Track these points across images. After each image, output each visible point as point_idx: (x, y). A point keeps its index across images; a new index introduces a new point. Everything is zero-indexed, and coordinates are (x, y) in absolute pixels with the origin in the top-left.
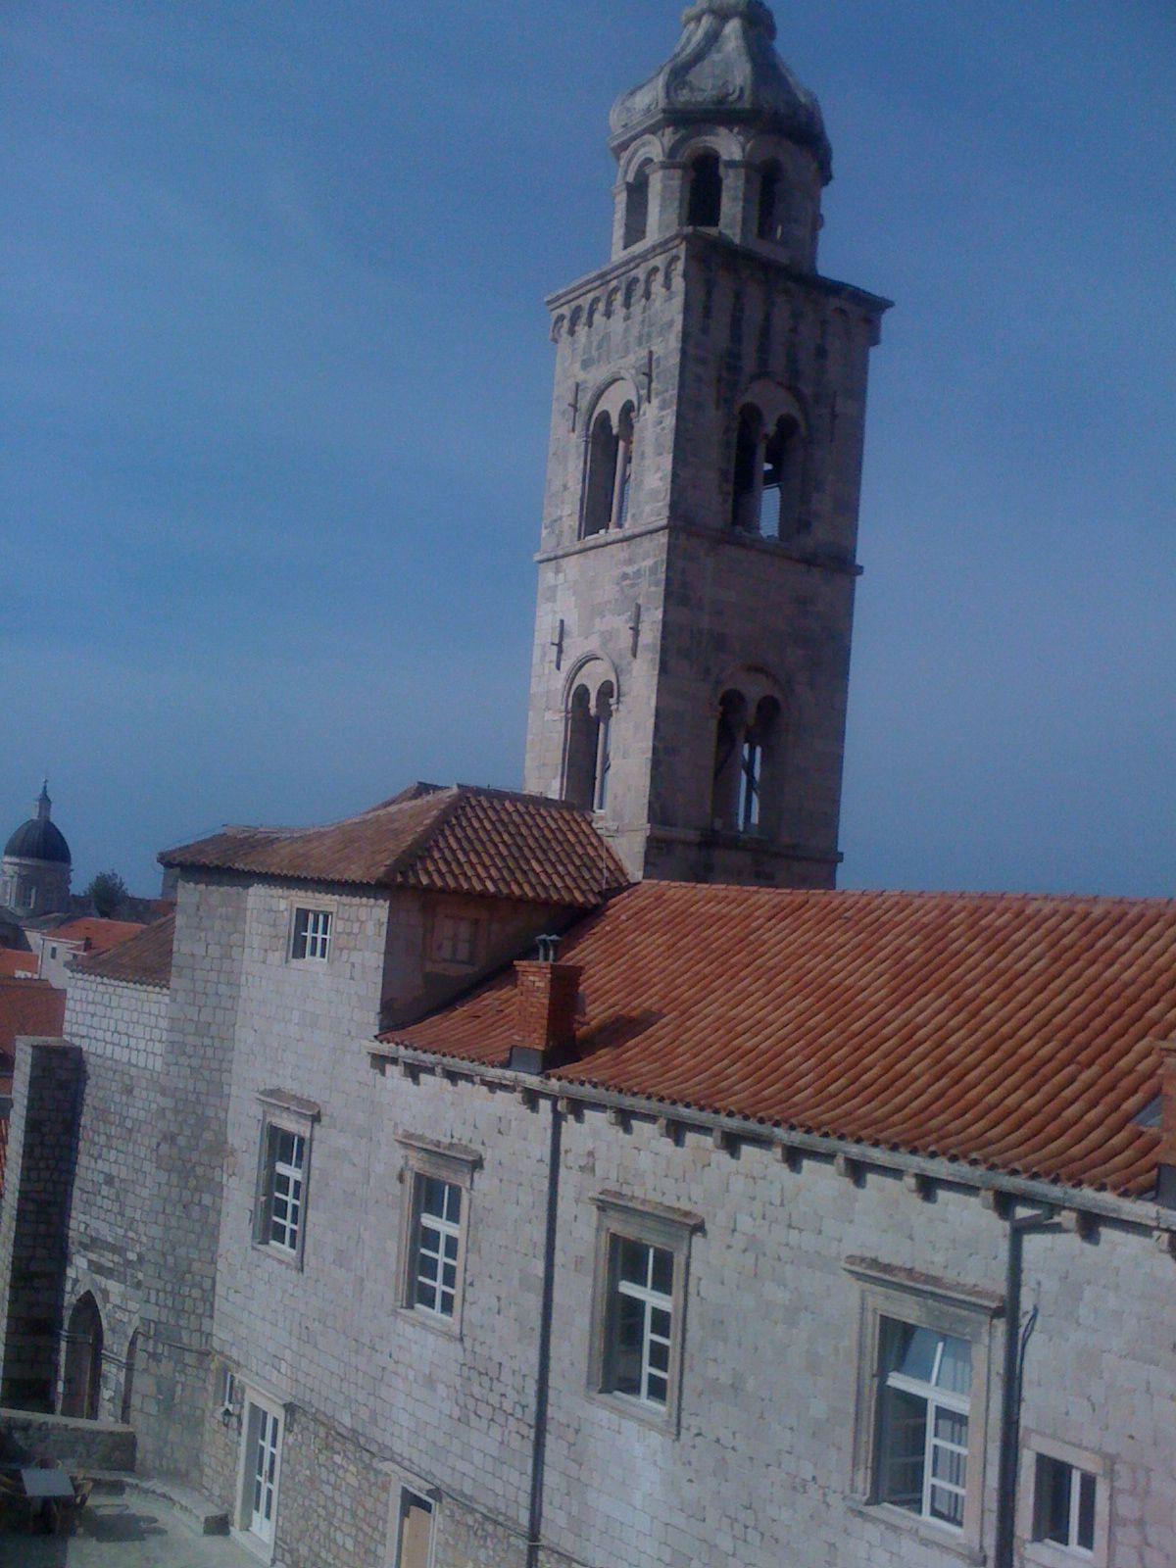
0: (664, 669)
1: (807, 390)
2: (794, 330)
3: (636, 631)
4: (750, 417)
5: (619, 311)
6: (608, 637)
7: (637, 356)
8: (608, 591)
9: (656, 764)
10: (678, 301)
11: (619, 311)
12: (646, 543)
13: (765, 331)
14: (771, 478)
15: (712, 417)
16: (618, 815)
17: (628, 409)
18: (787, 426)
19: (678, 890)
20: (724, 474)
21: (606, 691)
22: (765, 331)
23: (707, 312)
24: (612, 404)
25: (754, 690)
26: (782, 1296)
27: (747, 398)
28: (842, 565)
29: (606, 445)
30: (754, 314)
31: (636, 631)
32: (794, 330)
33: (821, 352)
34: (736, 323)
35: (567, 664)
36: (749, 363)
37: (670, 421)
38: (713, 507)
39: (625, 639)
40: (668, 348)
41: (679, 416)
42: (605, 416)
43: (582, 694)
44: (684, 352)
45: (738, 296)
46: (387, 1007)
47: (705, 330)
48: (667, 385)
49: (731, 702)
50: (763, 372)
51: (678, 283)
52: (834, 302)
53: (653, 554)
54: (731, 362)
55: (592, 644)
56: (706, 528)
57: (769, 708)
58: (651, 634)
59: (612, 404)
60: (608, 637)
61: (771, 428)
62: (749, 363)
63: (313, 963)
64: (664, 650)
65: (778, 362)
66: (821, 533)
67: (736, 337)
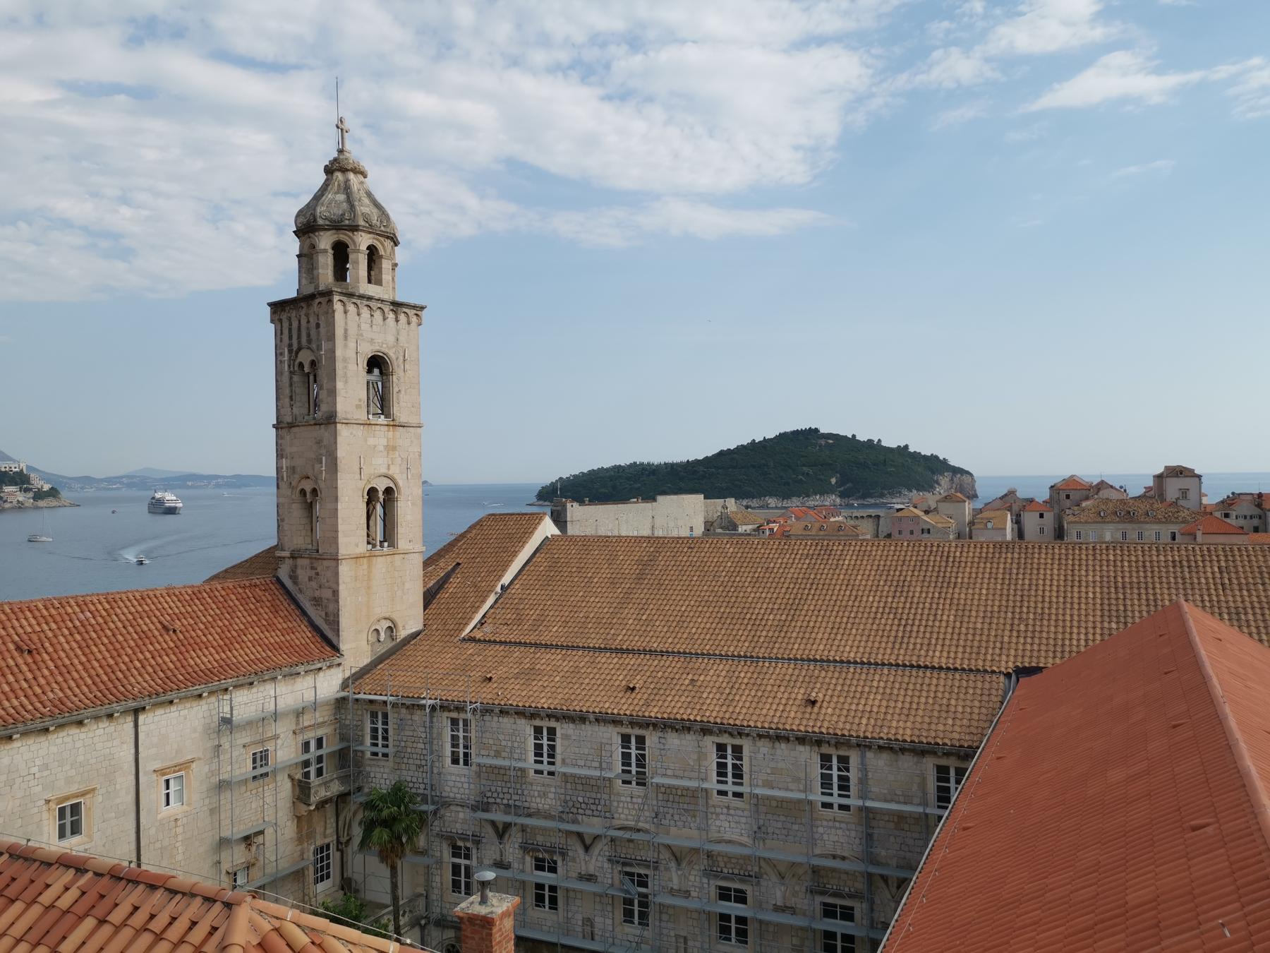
1: (314, 346)
4: (301, 365)
18: (313, 363)
30: (295, 325)
33: (318, 326)
34: (290, 330)
45: (289, 319)
52: (317, 301)
57: (314, 492)
67: (290, 338)
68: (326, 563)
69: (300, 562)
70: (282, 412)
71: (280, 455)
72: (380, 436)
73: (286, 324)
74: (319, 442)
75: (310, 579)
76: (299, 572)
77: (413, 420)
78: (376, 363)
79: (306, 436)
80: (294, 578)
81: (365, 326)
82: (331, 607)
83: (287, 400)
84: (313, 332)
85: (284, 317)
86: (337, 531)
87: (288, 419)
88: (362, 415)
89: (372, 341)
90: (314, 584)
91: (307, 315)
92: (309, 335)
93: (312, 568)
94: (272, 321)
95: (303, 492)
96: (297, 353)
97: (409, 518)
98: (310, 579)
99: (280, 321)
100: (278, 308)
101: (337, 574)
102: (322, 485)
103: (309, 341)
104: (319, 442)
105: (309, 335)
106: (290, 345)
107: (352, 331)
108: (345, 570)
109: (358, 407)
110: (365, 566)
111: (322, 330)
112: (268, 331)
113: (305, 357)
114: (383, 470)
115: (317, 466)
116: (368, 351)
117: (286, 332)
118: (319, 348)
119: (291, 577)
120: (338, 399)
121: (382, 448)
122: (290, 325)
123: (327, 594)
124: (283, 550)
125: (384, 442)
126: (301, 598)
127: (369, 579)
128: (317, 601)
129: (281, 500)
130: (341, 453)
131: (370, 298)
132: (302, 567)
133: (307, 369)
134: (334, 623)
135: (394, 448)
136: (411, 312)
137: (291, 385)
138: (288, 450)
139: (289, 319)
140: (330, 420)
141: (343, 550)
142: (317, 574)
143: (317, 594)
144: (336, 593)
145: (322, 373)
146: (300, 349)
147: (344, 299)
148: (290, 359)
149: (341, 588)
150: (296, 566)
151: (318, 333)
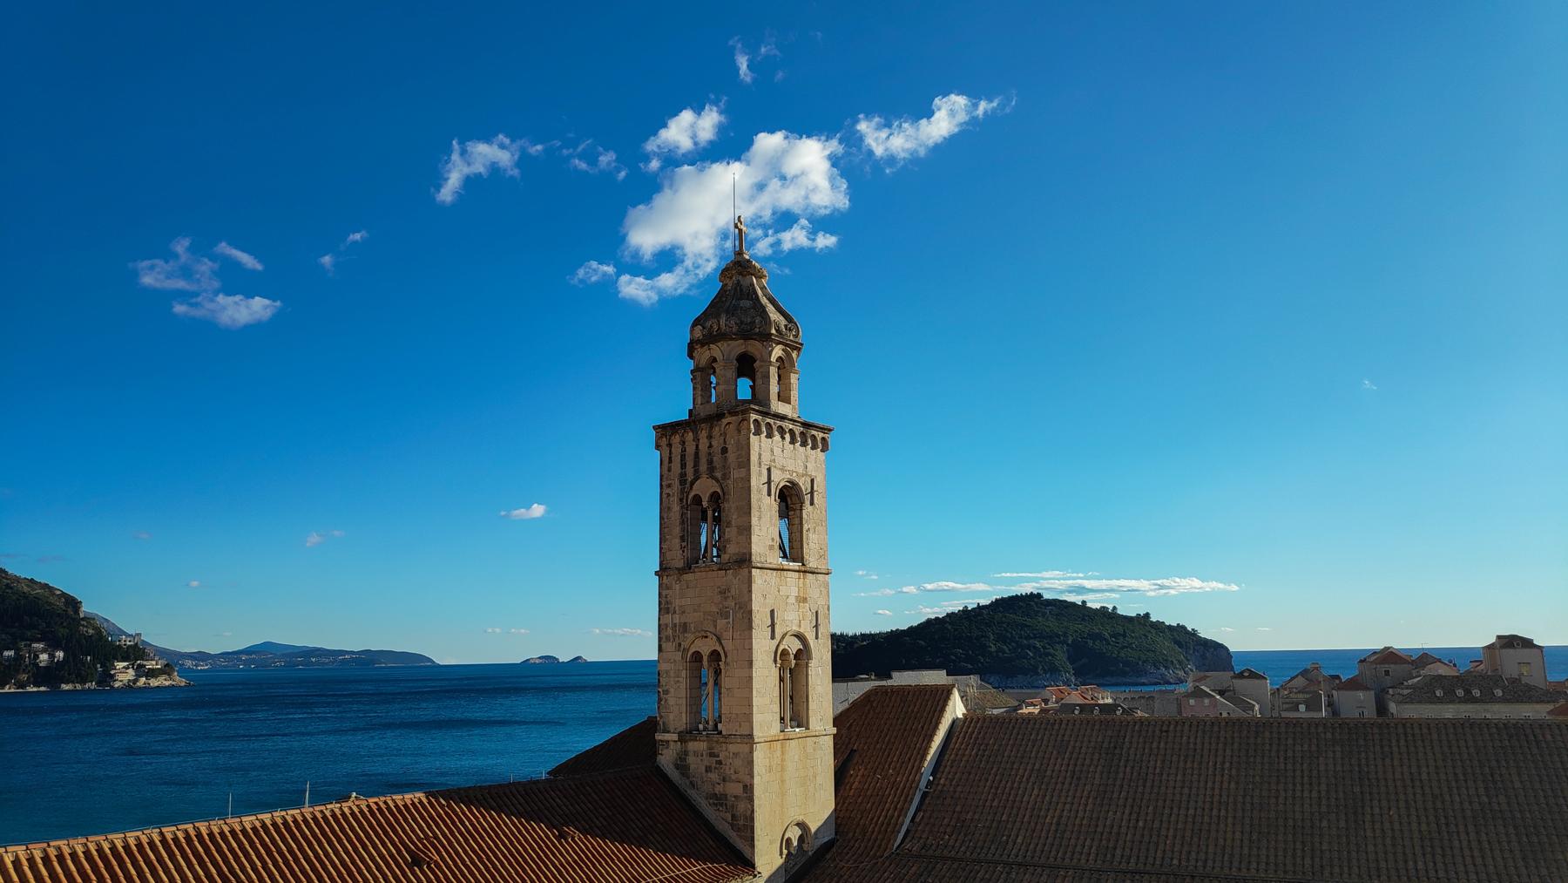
1: (718, 475)
2: (710, 446)
13: (697, 455)
18: (715, 498)
22: (697, 455)
23: (670, 461)
27: (692, 494)
30: (691, 449)
32: (710, 446)
33: (725, 450)
34: (683, 457)
45: (683, 443)
52: (725, 421)
54: (683, 481)
57: (715, 656)
65: (703, 467)
66: (732, 549)
67: (683, 466)
68: (733, 748)
69: (692, 746)
70: (669, 556)
71: (664, 608)
72: (792, 584)
73: (677, 450)
74: (724, 593)
75: (708, 769)
76: (691, 759)
77: (823, 568)
78: (790, 500)
79: (701, 589)
80: (681, 765)
81: (777, 451)
82: (742, 806)
84: (717, 459)
85: (676, 439)
86: (750, 706)
87: (680, 564)
88: (776, 559)
89: (783, 469)
90: (713, 776)
91: (710, 437)
92: (710, 462)
93: (712, 755)
94: (658, 447)
95: (697, 657)
96: (692, 484)
97: (819, 689)
98: (708, 769)
99: (670, 445)
100: (666, 432)
101: (751, 763)
102: (728, 645)
103: (711, 469)
104: (724, 593)
105: (710, 462)
106: (683, 476)
107: (766, 458)
108: (760, 756)
109: (771, 547)
110: (779, 753)
111: (731, 456)
112: (651, 461)
113: (704, 488)
114: (795, 628)
115: (721, 623)
116: (779, 479)
117: (677, 459)
118: (725, 476)
119: (677, 767)
120: (754, 538)
121: (792, 600)
122: (684, 450)
123: (734, 789)
124: (666, 731)
125: (794, 592)
126: (692, 793)
127: (783, 769)
128: (719, 800)
130: (755, 607)
131: (783, 418)
133: (705, 504)
134: (746, 827)
135: (805, 600)
136: (820, 435)
137: (683, 523)
138: (677, 603)
139: (683, 443)
140: (744, 561)
141: (758, 734)
142: (720, 763)
143: (719, 789)
144: (748, 789)
145: (730, 506)
146: (697, 478)
147: (759, 418)
148: (682, 491)
149: (757, 780)
150: (686, 753)
151: (726, 459)
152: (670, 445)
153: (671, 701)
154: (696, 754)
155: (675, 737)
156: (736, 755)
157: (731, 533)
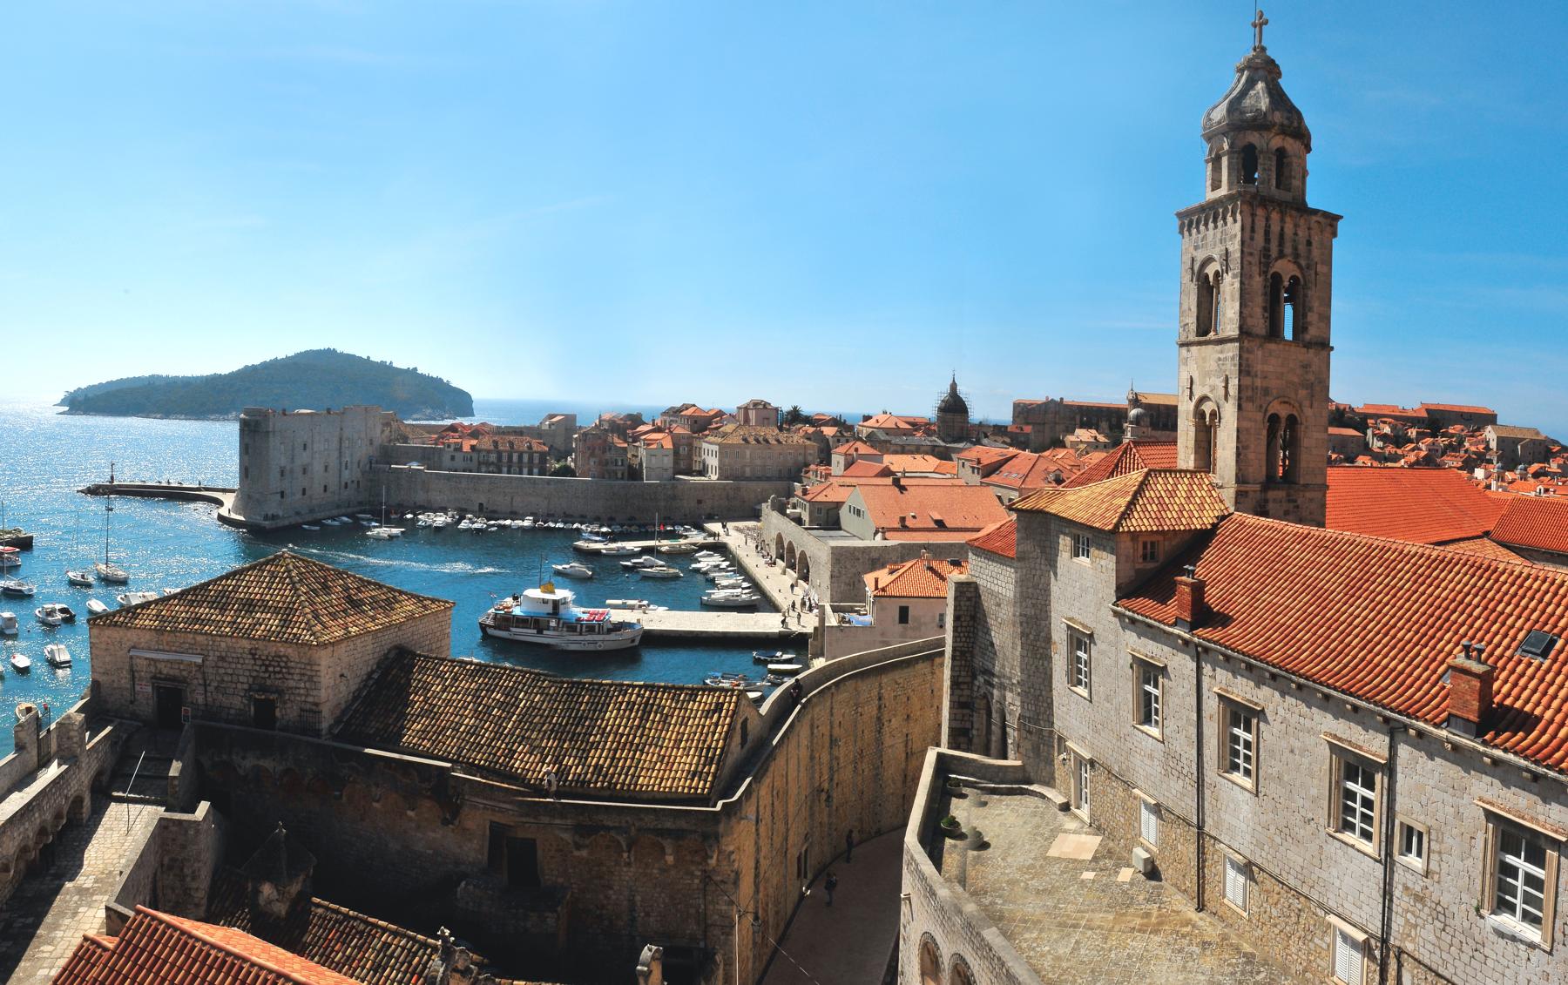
0: (1240, 408)
3: (1226, 387)
4: (1277, 278)
5: (1211, 225)
6: (1213, 389)
7: (1216, 253)
8: (1212, 365)
9: (1238, 454)
10: (1239, 224)
11: (1211, 225)
12: (1229, 345)
14: (1286, 300)
15: (1258, 282)
16: (1222, 478)
17: (1217, 274)
19: (1251, 519)
20: (1265, 309)
21: (1213, 414)
23: (1253, 230)
24: (1210, 271)
25: (1284, 412)
26: (1297, 744)
28: (1324, 346)
29: (1207, 290)
30: (1275, 228)
31: (1226, 387)
34: (1267, 233)
35: (1195, 400)
36: (1274, 252)
37: (1237, 285)
38: (1259, 324)
39: (1222, 392)
40: (1235, 247)
41: (1242, 283)
42: (1207, 276)
43: (1203, 415)
44: (1242, 252)
45: (1268, 219)
46: (1118, 588)
47: (1252, 239)
48: (1235, 266)
49: (1274, 419)
50: (1281, 255)
51: (1239, 217)
53: (1232, 350)
54: (1266, 252)
55: (1206, 391)
56: (1257, 334)
57: (1292, 421)
58: (1233, 391)
59: (1210, 271)
60: (1213, 389)
61: (1286, 284)
62: (1274, 252)
63: (1083, 559)
64: (1240, 399)
65: (1288, 250)
66: (1313, 332)
67: (1267, 240)
69: (1271, 495)
70: (1250, 321)
83: (1258, 311)
84: (1302, 248)
92: (1295, 248)
99: (1253, 215)
105: (1295, 248)
129: (1246, 424)
132: (1274, 501)
139: (1268, 219)
150: (1266, 501)
152: (1253, 215)
153: (1251, 456)
154: (1274, 501)
155: (1258, 487)
156: (1311, 500)
157: (1312, 317)
